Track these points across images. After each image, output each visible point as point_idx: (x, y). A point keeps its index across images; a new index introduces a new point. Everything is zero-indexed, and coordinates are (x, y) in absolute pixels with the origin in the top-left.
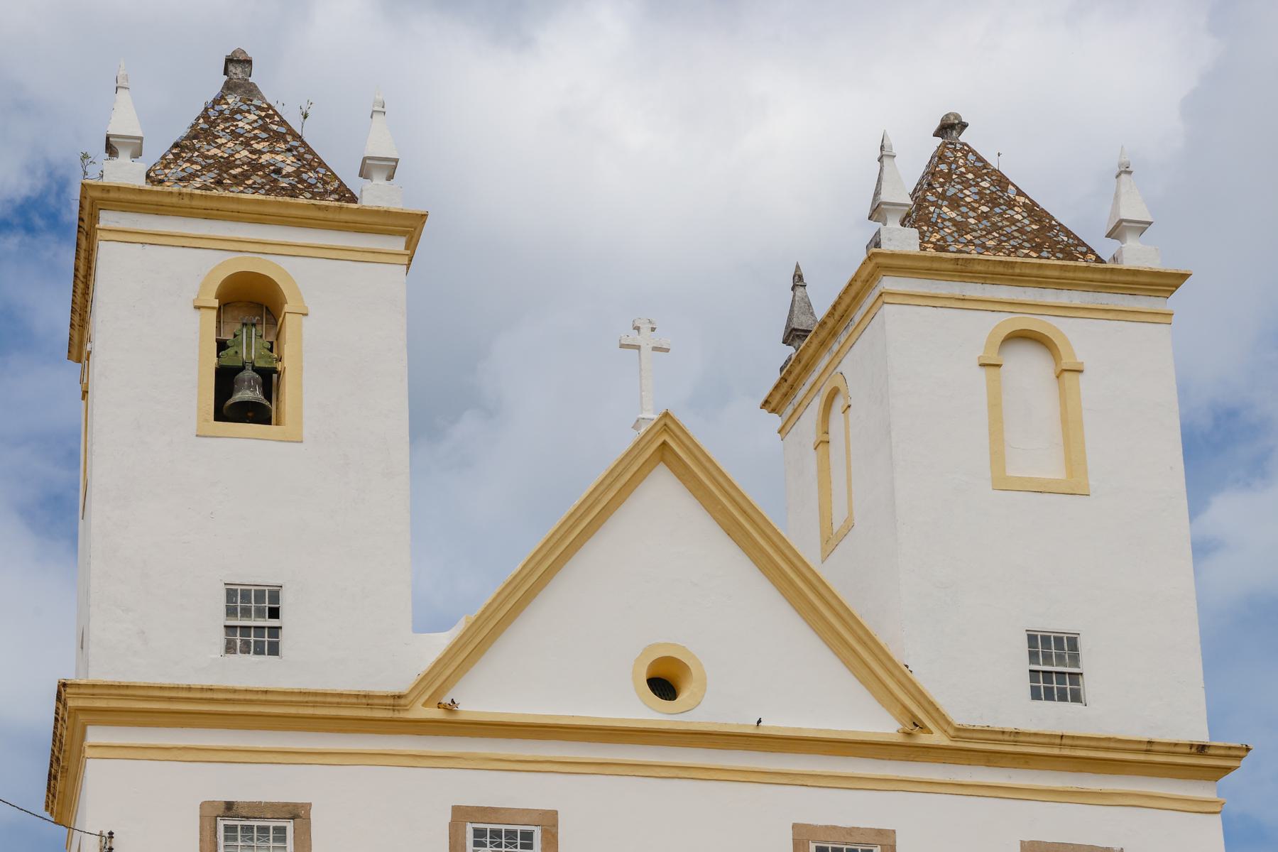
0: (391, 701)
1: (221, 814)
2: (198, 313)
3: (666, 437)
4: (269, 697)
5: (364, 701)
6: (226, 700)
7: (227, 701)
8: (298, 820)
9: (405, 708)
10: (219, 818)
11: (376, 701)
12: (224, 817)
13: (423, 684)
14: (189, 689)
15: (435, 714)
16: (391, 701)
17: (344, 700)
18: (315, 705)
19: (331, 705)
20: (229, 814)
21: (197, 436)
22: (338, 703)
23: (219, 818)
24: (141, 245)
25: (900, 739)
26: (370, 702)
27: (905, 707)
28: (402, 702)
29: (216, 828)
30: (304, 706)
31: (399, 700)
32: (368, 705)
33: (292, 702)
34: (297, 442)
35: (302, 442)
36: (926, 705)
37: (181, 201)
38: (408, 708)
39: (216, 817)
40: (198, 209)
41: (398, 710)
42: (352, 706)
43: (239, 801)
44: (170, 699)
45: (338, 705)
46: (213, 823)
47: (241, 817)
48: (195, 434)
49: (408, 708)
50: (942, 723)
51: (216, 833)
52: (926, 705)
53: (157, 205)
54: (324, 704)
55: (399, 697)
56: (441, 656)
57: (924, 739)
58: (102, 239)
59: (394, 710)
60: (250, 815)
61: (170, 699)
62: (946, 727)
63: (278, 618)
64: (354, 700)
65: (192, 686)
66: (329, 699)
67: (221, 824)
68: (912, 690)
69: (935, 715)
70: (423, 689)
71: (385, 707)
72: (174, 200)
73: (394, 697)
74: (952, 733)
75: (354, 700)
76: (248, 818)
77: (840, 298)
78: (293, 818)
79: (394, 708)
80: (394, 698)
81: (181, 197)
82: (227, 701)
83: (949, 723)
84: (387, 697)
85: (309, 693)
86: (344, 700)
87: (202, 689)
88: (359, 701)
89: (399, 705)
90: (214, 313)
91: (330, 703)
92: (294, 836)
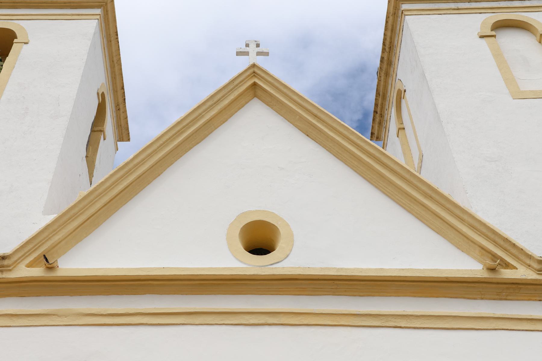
3: (254, 74)
13: (30, 246)
15: (38, 272)
25: (483, 274)
27: (483, 248)
28: (6, 262)
36: (502, 243)
38: (10, 268)
49: (10, 268)
50: (523, 258)
52: (502, 243)
57: (507, 274)
62: (528, 262)
68: (484, 230)
69: (514, 251)
74: (536, 266)
77: (384, 34)
83: (530, 257)
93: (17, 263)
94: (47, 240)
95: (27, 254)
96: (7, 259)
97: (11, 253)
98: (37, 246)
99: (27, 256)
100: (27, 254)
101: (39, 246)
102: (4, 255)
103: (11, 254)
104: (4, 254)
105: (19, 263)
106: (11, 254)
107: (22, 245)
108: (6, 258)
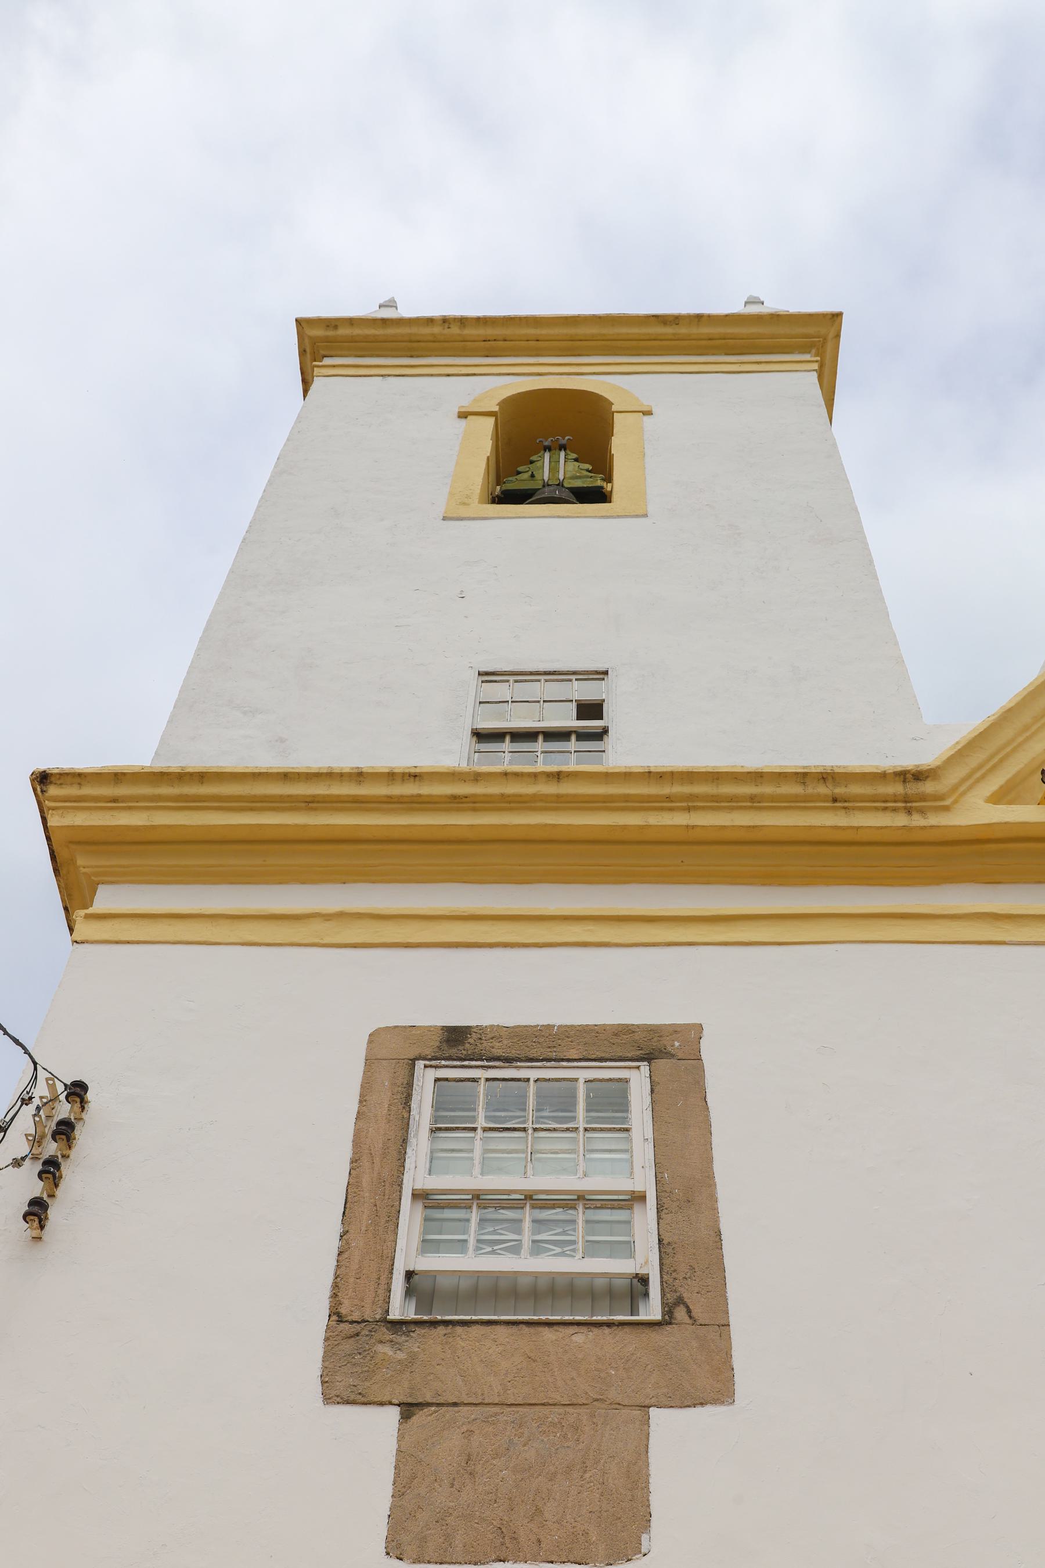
0: (897, 788)
1: (428, 1052)
2: (463, 422)
4: (567, 788)
5: (823, 790)
6: (455, 798)
7: (456, 803)
8: (661, 1063)
9: (939, 803)
10: (420, 1064)
11: (856, 789)
12: (434, 1059)
14: (359, 776)
16: (897, 788)
17: (768, 789)
18: (690, 803)
19: (732, 803)
20: (453, 1052)
21: (444, 519)
22: (752, 798)
23: (420, 1064)
24: (381, 378)
26: (839, 791)
28: (928, 787)
29: (410, 1085)
30: (662, 809)
31: (920, 784)
32: (835, 800)
33: (627, 798)
34: (637, 516)
35: (645, 516)
37: (447, 331)
38: (947, 802)
39: (413, 1061)
40: (474, 341)
41: (922, 811)
42: (793, 803)
43: (485, 1022)
44: (311, 804)
45: (754, 803)
46: (403, 1072)
47: (488, 1060)
48: (442, 517)
49: (947, 802)
51: (409, 1097)
53: (411, 341)
54: (716, 803)
55: (918, 776)
56: (1012, 704)
58: (319, 374)
59: (909, 811)
60: (513, 1053)
61: (311, 804)
63: (602, 719)
64: (796, 789)
65: (364, 770)
66: (728, 789)
67: (425, 1079)
70: (980, 767)
71: (884, 804)
72: (436, 330)
73: (904, 776)
75: (796, 789)
76: (508, 1061)
78: (649, 1058)
79: (908, 804)
80: (904, 781)
81: (446, 325)
82: (456, 803)
84: (882, 776)
85: (672, 773)
86: (768, 789)
87: (391, 776)
88: (810, 790)
89: (923, 798)
90: (491, 421)
91: (732, 799)
92: (653, 1102)
93: (961, 790)
94: (1014, 750)
95: (978, 775)
96: (929, 779)
97: (938, 763)
98: (996, 760)
99: (978, 781)
100: (978, 775)
101: (1001, 761)
102: (919, 769)
103: (939, 765)
104: (918, 766)
105: (964, 793)
106: (938, 767)
107: (959, 747)
108: (927, 777)
